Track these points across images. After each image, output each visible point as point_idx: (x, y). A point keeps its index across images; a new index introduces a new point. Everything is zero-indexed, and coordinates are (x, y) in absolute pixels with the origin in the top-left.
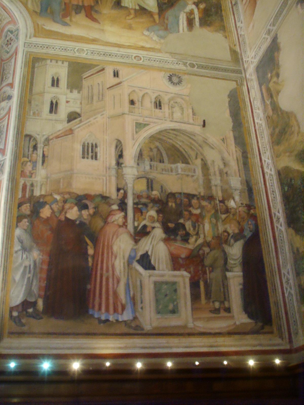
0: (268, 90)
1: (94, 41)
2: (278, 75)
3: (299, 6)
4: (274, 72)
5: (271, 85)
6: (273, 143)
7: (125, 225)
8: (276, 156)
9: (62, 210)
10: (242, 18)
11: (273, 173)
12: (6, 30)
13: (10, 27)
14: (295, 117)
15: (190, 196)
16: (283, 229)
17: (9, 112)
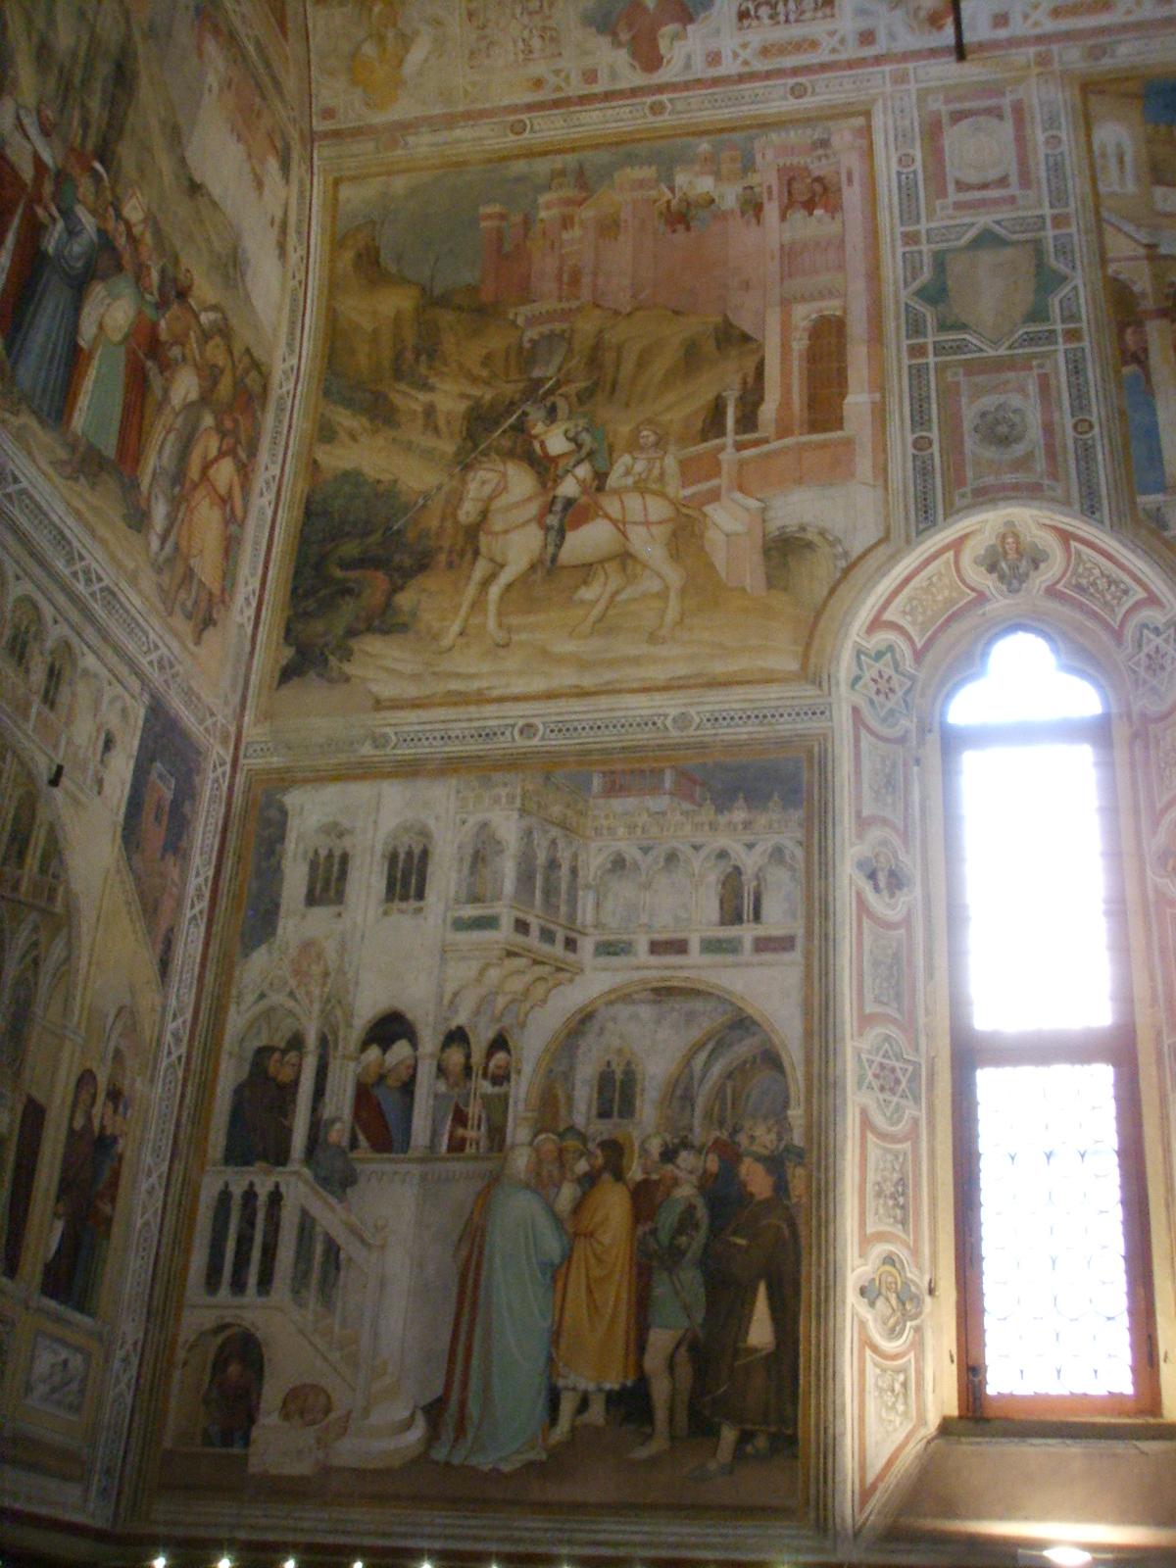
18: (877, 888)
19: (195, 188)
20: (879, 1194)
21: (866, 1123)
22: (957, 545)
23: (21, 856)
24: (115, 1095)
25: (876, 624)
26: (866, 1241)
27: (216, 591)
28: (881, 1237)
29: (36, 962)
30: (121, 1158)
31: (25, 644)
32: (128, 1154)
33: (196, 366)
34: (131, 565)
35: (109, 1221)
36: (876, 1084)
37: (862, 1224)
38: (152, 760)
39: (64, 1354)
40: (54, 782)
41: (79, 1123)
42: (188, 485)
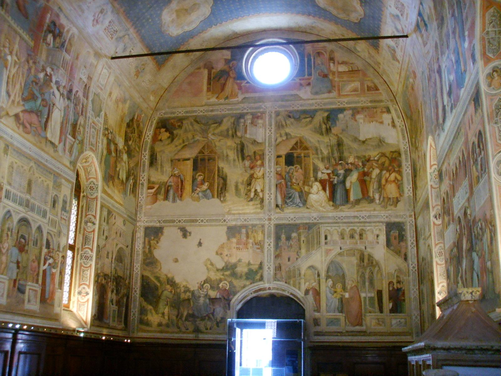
0: (149, 242)
1: (112, 198)
2: (158, 242)
3: (179, 230)
4: (156, 239)
5: (151, 242)
6: (143, 263)
7: (110, 288)
8: (143, 269)
9: (102, 280)
10: (144, 195)
11: (139, 273)
12: (91, 180)
13: (94, 180)
14: (160, 264)
15: (121, 277)
16: (138, 296)
17: (94, 231)
18: (437, 219)
19: (364, 142)
20: (440, 275)
21: (437, 263)
22: (431, 146)
23: (363, 262)
24: (399, 282)
25: (431, 166)
26: (438, 284)
27: (398, 195)
28: (441, 283)
29: (372, 273)
30: (404, 290)
31: (353, 235)
32: (406, 289)
33: (377, 167)
34: (373, 209)
35: (404, 300)
36: (438, 256)
37: (438, 281)
38: (390, 231)
39: (398, 320)
40: (366, 249)
41: (391, 289)
42: (382, 187)
